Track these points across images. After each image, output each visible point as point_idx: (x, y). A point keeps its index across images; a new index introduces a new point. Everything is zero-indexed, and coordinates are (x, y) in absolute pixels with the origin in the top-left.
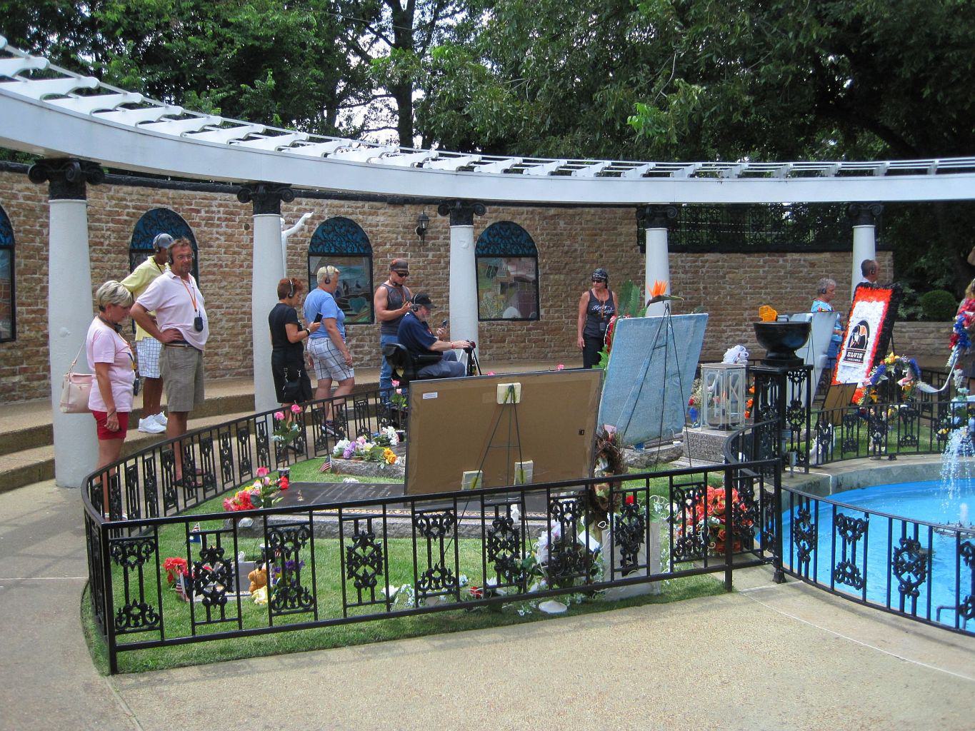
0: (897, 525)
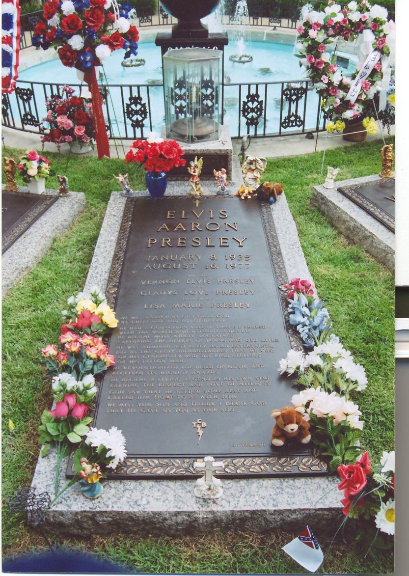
0: (48, 87)
